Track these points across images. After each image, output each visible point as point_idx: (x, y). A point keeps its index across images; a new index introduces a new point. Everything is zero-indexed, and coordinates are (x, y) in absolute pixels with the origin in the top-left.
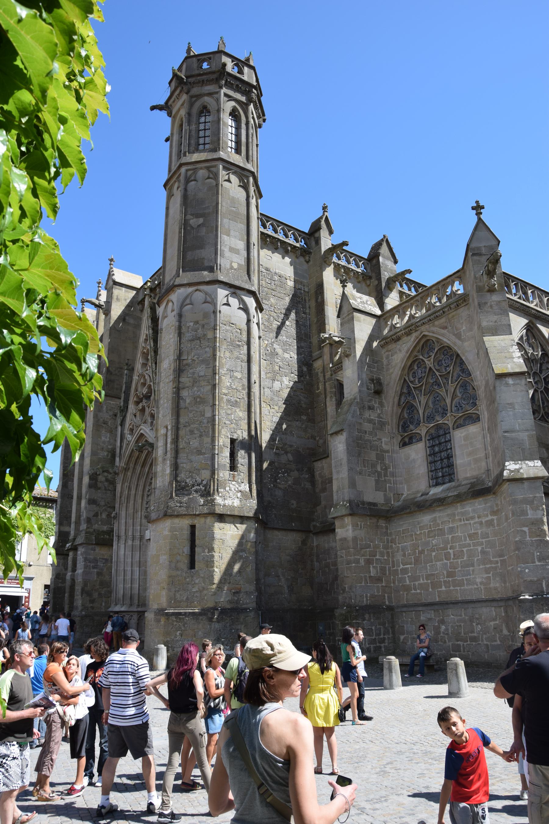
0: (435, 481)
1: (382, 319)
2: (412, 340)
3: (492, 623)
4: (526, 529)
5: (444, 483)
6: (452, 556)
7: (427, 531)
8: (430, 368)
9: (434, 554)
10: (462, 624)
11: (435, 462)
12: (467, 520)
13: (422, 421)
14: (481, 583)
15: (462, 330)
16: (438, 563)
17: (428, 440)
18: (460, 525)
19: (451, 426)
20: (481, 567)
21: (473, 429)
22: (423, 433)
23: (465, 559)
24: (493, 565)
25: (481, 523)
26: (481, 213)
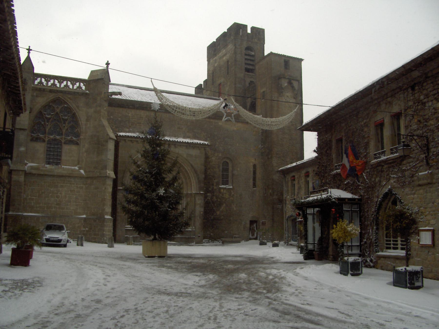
3: (77, 225)
6: (60, 197)
9: (50, 194)
11: (50, 154)
12: (70, 184)
20: (74, 203)
21: (74, 147)
22: (47, 140)
25: (77, 187)
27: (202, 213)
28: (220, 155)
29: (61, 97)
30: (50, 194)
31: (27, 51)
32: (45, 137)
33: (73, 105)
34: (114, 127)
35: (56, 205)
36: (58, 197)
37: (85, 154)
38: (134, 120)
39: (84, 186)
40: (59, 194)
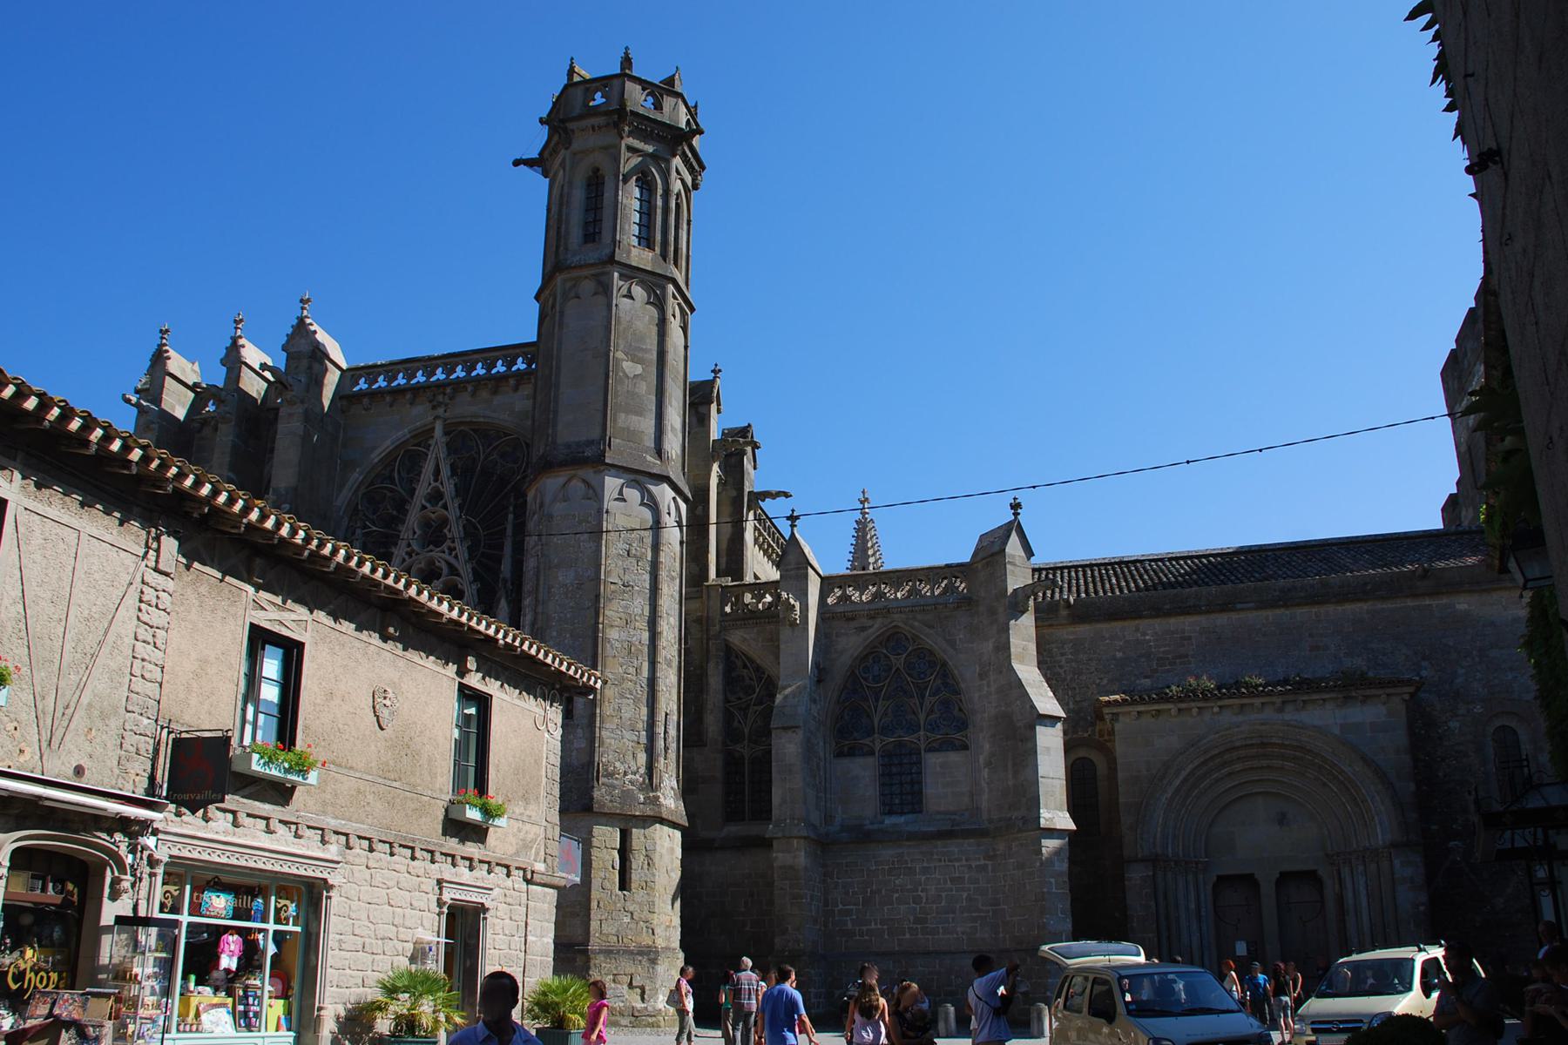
0: (887, 808)
1: (826, 582)
2: (876, 626)
4: (1053, 880)
5: (902, 813)
6: (924, 901)
7: (887, 867)
8: (898, 669)
9: (896, 895)
10: (935, 977)
12: (949, 861)
13: (876, 731)
14: (963, 933)
15: (958, 637)
16: (902, 907)
17: (882, 756)
18: (939, 866)
19: (923, 747)
20: (966, 915)
21: (954, 757)
22: (878, 747)
23: (943, 904)
24: (982, 914)
25: (970, 867)
26: (1019, 514)
27: (1422, 908)
28: (1478, 709)
29: (900, 624)
30: (896, 895)
31: (790, 522)
32: (873, 742)
33: (933, 641)
34: (1105, 681)
35: (914, 923)
36: (917, 900)
37: (985, 773)
38: (1162, 649)
39: (990, 863)
40: (920, 893)
